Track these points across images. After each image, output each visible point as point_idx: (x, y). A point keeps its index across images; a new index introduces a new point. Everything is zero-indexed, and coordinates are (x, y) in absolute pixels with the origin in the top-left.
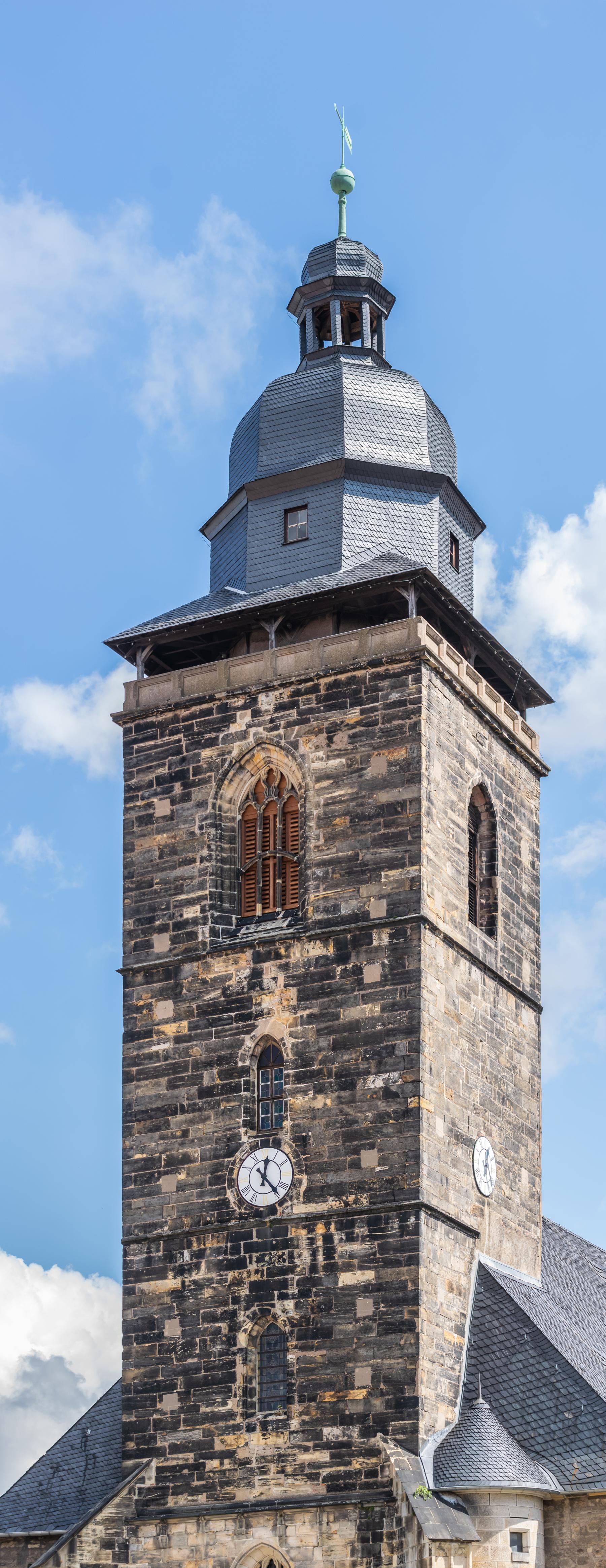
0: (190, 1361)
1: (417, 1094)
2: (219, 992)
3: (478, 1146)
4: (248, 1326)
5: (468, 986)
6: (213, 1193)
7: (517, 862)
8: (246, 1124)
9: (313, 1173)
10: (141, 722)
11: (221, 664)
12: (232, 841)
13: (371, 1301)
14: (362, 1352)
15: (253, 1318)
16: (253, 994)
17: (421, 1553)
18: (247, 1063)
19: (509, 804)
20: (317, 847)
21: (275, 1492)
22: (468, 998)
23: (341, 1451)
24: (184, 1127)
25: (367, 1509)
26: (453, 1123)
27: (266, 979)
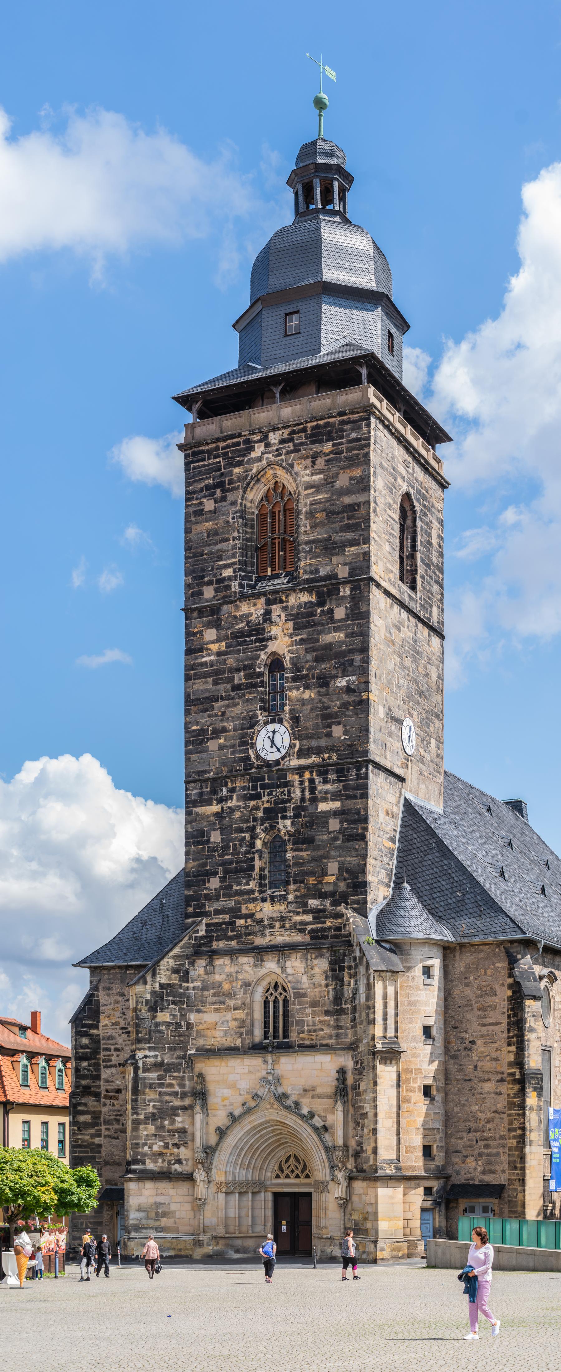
0: (226, 857)
1: (367, 690)
2: (244, 624)
3: (404, 724)
4: (263, 835)
5: (399, 622)
6: (241, 752)
7: (430, 543)
8: (261, 708)
9: (303, 739)
10: (196, 449)
11: (245, 413)
12: (252, 527)
13: (337, 821)
14: (333, 853)
15: (265, 831)
16: (266, 625)
17: (368, 978)
18: (262, 669)
19: (425, 506)
20: (305, 531)
21: (279, 940)
22: (399, 629)
23: (319, 914)
24: (223, 709)
25: (335, 951)
26: (389, 709)
27: (274, 616)
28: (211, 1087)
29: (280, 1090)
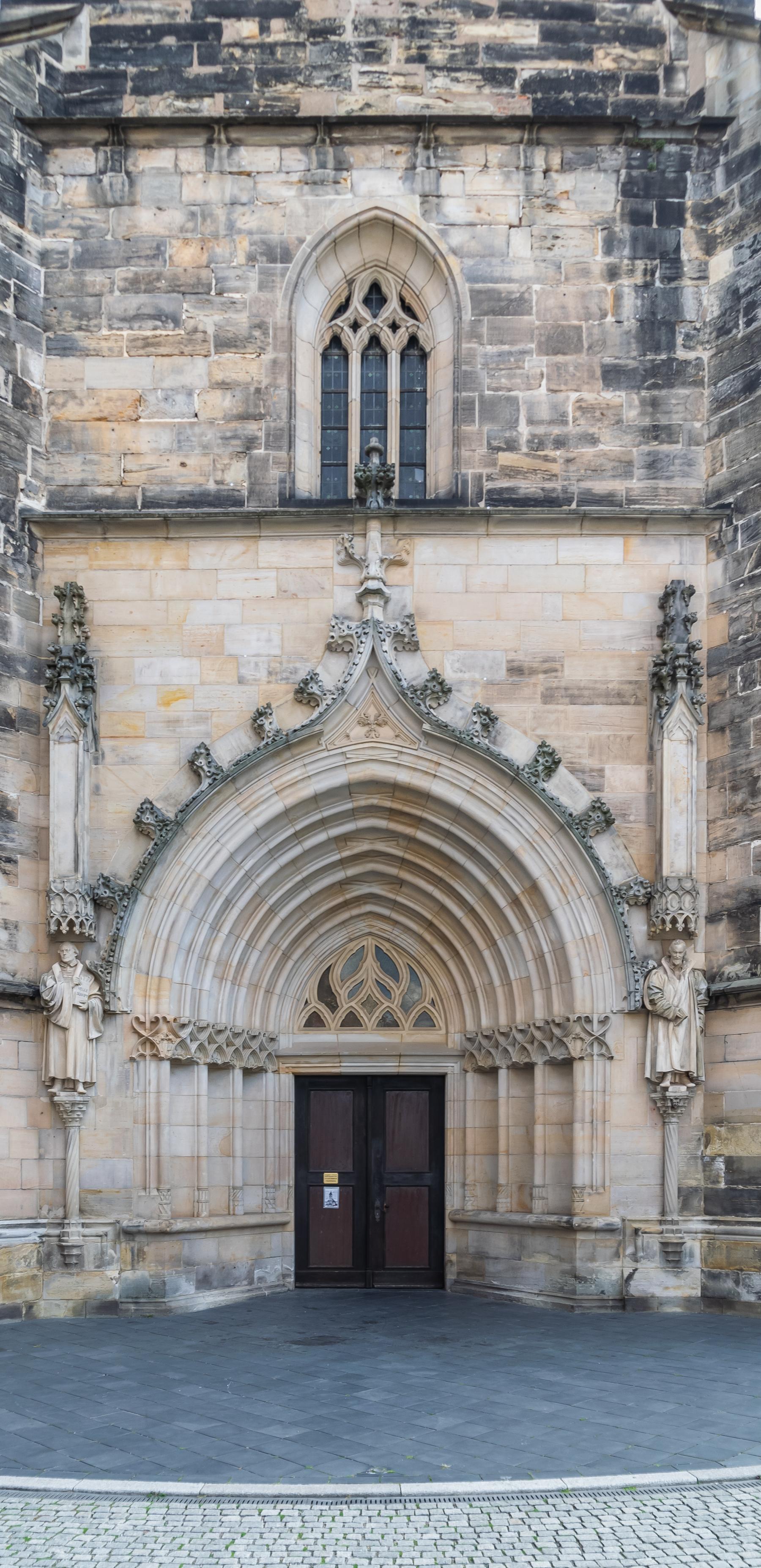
28: (110, 648)
29: (412, 669)
